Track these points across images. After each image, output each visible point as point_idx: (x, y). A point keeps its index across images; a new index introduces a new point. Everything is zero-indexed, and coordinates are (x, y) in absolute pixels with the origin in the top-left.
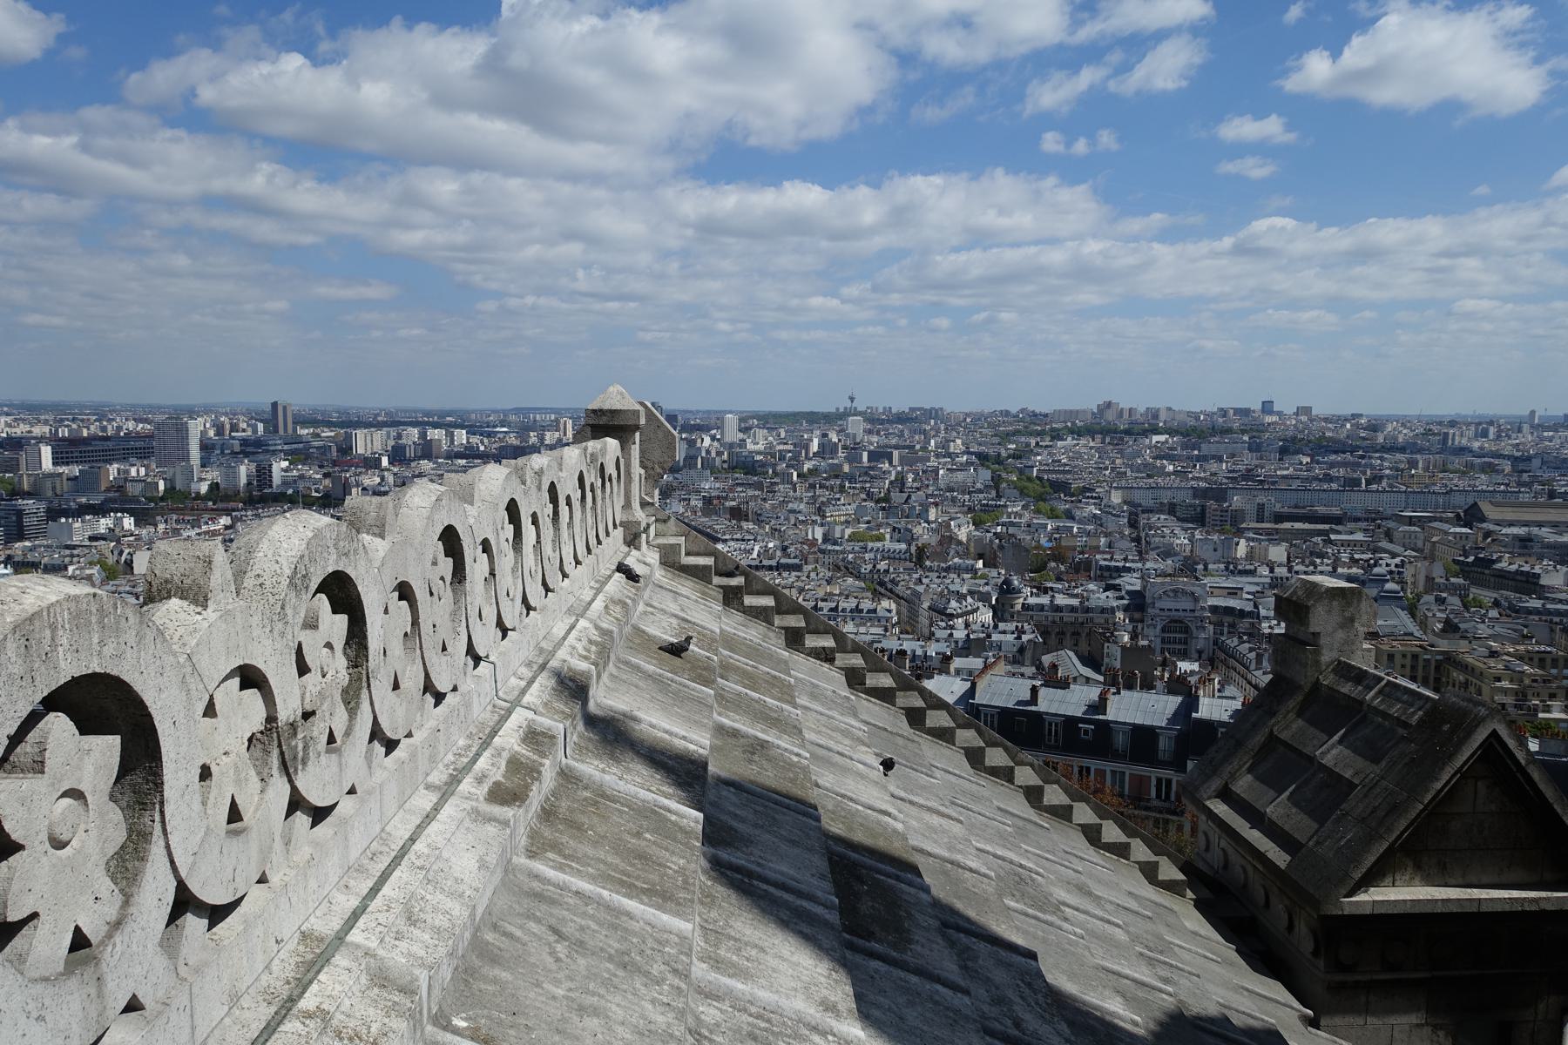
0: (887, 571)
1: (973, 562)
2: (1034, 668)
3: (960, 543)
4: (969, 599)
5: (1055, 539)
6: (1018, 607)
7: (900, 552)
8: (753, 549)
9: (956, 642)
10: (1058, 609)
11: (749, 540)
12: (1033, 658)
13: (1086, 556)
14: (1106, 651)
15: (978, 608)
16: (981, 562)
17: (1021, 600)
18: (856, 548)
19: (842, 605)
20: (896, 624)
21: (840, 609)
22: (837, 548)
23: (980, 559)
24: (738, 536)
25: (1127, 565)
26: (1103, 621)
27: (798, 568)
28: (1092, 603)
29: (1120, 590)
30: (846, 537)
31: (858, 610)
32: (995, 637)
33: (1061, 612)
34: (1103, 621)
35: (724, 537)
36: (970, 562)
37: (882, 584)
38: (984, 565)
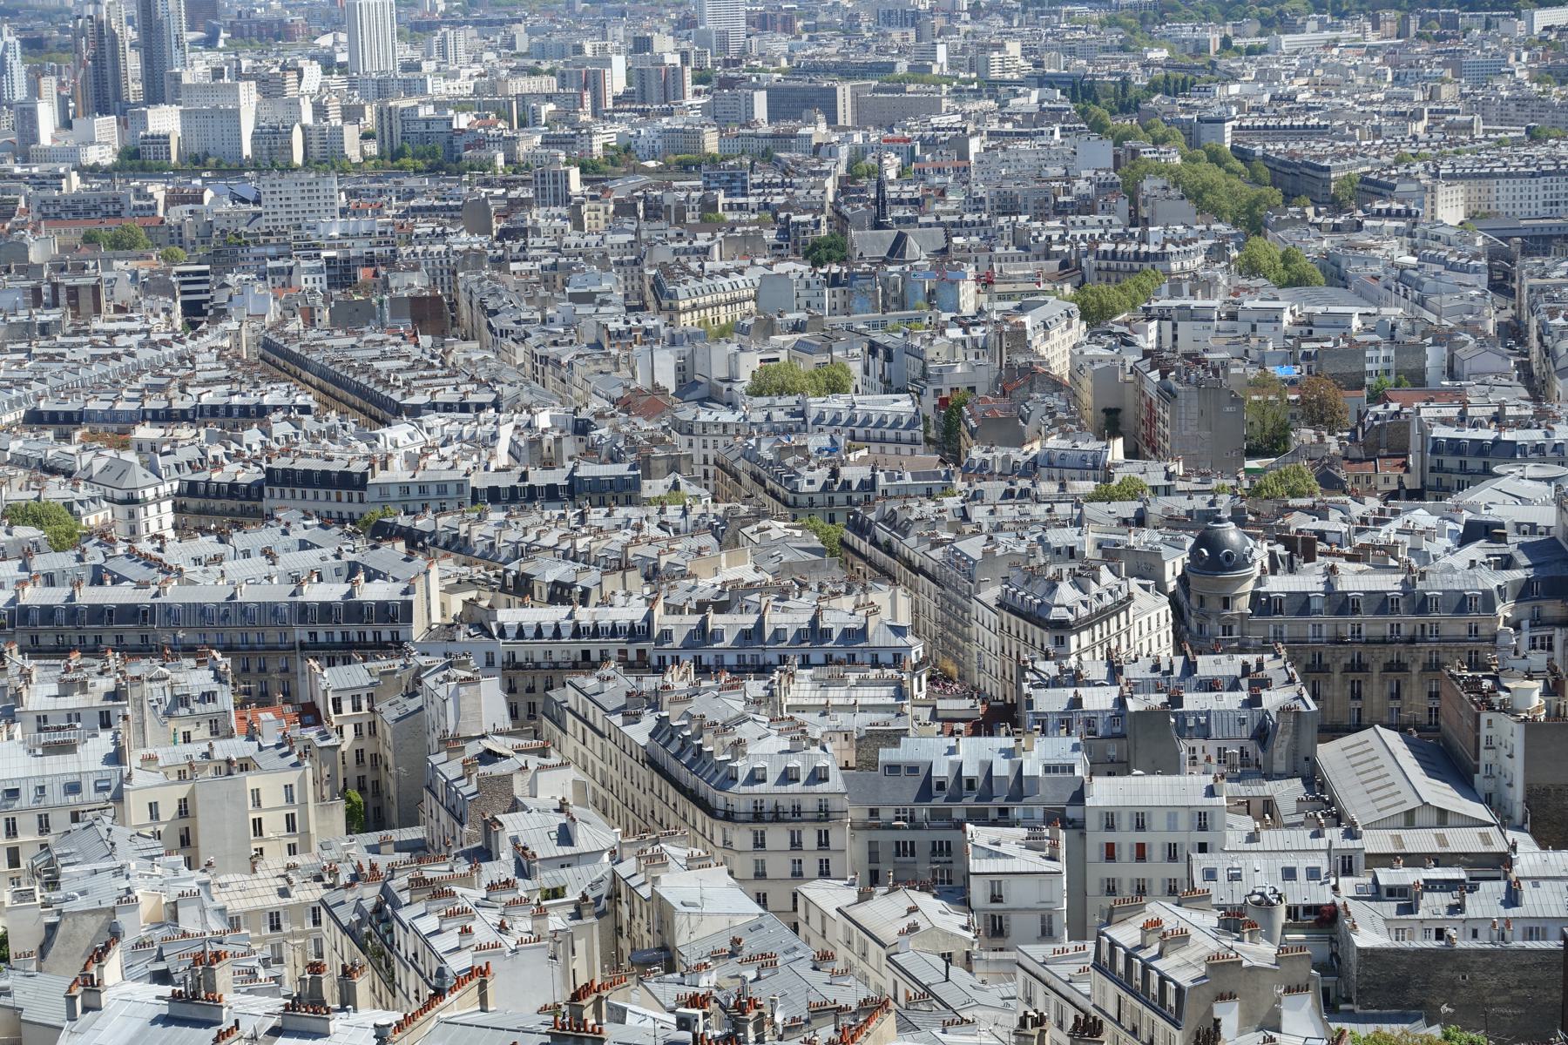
0: (869, 485)
1: (1095, 445)
2: (1298, 782)
3: (1056, 385)
4: (1106, 576)
5: (1307, 356)
6: (1243, 605)
7: (897, 423)
8: (495, 437)
9: (1089, 723)
10: (1343, 604)
11: (480, 407)
12: (1294, 753)
13: (1394, 407)
14: (1484, 732)
15: (1130, 597)
16: (1118, 444)
17: (1249, 586)
18: (778, 416)
19: (774, 620)
20: (922, 663)
21: (768, 632)
22: (726, 416)
23: (1114, 434)
24: (447, 395)
25: (1507, 436)
26: (1464, 631)
27: (622, 492)
28: (1434, 585)
29: (1502, 538)
30: (745, 377)
31: (815, 633)
32: (1193, 701)
33: (1356, 611)
34: (1464, 631)
35: (409, 401)
36: (1090, 445)
37: (861, 528)
38: (1127, 455)
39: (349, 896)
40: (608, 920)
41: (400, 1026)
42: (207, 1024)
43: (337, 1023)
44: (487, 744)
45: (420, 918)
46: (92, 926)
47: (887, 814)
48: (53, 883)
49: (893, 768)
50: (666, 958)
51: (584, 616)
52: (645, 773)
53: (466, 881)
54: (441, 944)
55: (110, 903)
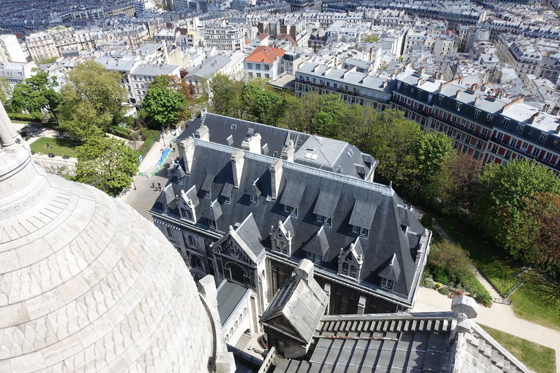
19: (542, 29)
21: (540, 31)
31: (549, 32)
39: (453, 62)
40: (492, 74)
41: (445, 83)
42: (418, 77)
43: (436, 81)
44: (483, 42)
45: (461, 67)
46: (414, 59)
47: (547, 66)
48: (411, 52)
49: (552, 58)
50: (499, 82)
51: (508, 23)
52: (508, 51)
53: (471, 63)
54: (463, 72)
55: (418, 56)
